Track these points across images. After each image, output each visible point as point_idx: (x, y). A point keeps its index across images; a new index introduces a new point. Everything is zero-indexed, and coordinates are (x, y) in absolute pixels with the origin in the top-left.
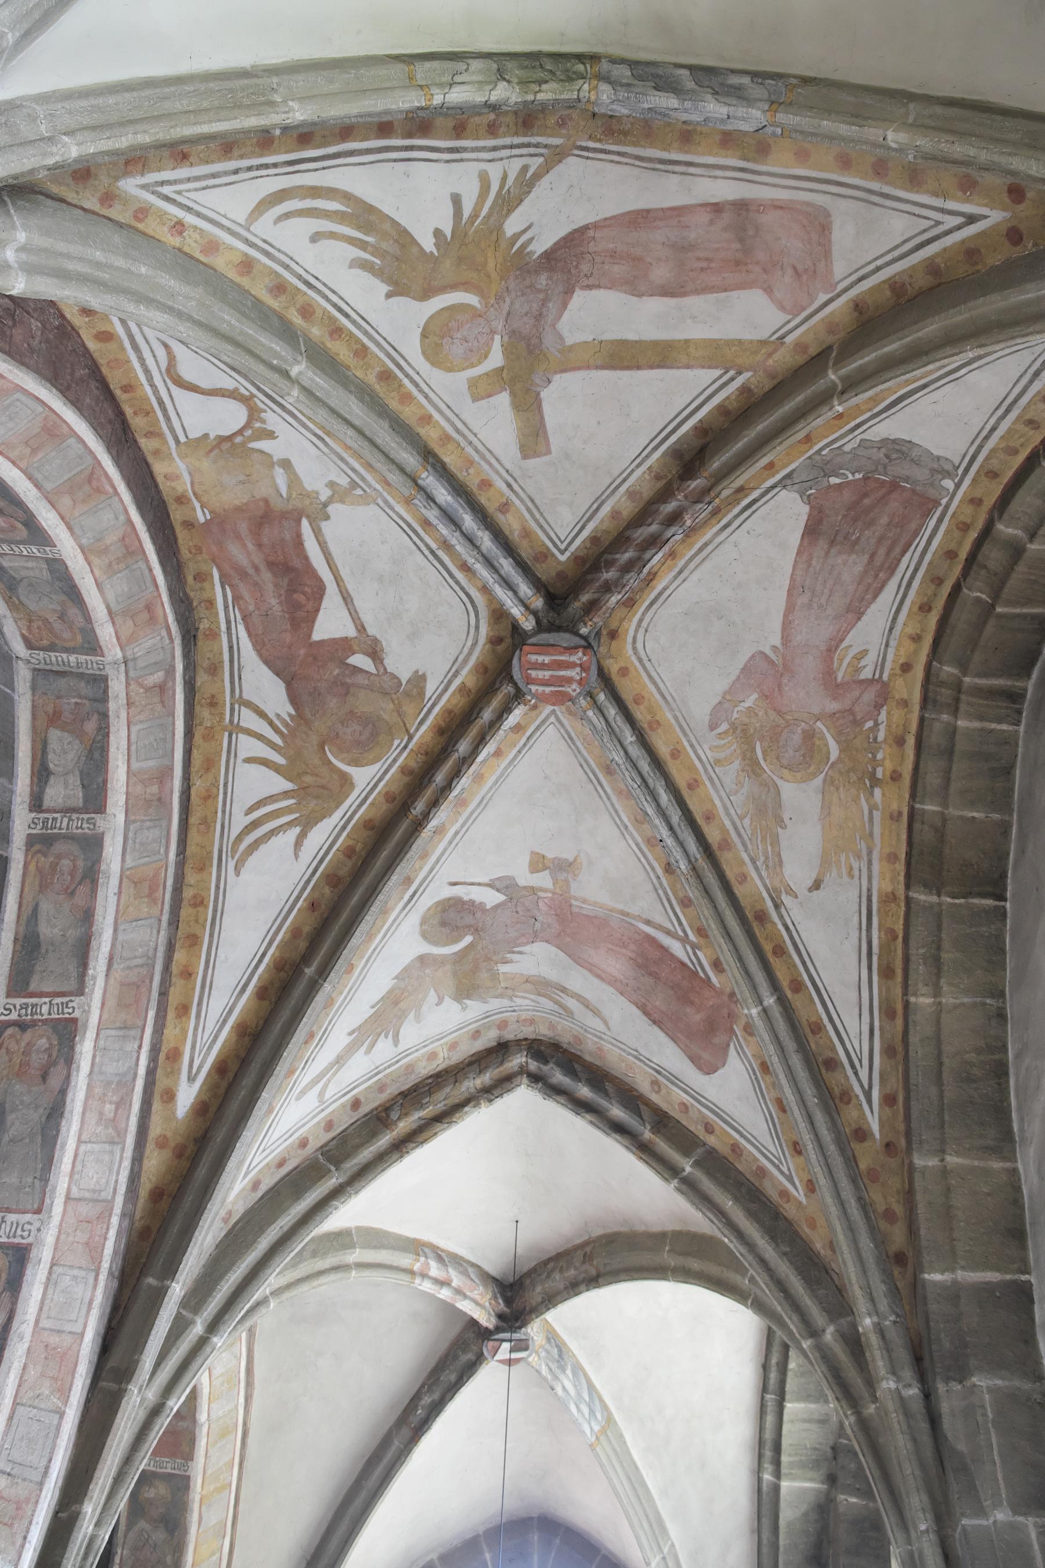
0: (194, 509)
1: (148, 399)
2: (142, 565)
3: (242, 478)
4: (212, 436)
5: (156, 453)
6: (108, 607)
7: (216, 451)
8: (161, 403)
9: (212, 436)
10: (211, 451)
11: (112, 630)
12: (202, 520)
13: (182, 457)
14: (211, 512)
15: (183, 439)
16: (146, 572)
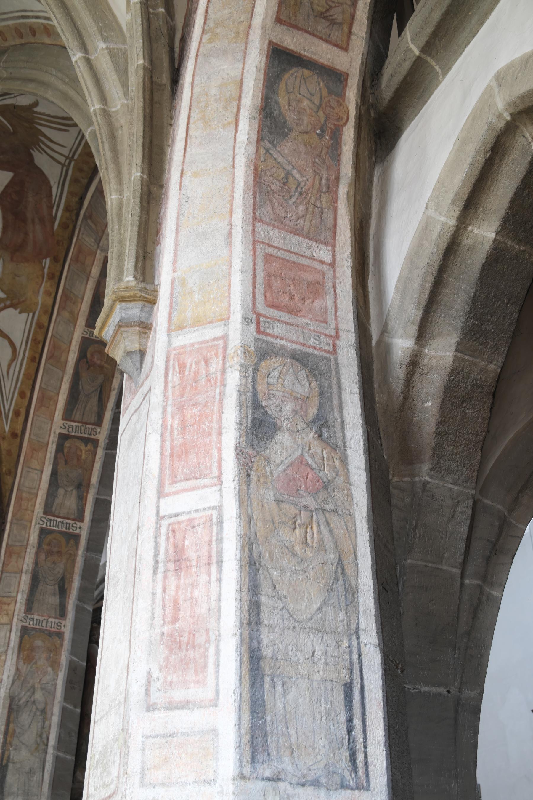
0: (49, 268)
1: (30, 349)
2: (67, 286)
3: (17, 279)
4: (18, 310)
5: (45, 312)
6: (87, 284)
7: (21, 300)
8: (27, 342)
9: (18, 310)
10: (23, 301)
11: (93, 270)
12: (48, 260)
13: (37, 304)
14: (42, 263)
15: (31, 314)
16: (68, 279)
